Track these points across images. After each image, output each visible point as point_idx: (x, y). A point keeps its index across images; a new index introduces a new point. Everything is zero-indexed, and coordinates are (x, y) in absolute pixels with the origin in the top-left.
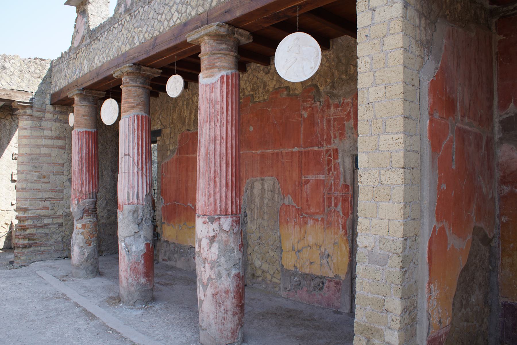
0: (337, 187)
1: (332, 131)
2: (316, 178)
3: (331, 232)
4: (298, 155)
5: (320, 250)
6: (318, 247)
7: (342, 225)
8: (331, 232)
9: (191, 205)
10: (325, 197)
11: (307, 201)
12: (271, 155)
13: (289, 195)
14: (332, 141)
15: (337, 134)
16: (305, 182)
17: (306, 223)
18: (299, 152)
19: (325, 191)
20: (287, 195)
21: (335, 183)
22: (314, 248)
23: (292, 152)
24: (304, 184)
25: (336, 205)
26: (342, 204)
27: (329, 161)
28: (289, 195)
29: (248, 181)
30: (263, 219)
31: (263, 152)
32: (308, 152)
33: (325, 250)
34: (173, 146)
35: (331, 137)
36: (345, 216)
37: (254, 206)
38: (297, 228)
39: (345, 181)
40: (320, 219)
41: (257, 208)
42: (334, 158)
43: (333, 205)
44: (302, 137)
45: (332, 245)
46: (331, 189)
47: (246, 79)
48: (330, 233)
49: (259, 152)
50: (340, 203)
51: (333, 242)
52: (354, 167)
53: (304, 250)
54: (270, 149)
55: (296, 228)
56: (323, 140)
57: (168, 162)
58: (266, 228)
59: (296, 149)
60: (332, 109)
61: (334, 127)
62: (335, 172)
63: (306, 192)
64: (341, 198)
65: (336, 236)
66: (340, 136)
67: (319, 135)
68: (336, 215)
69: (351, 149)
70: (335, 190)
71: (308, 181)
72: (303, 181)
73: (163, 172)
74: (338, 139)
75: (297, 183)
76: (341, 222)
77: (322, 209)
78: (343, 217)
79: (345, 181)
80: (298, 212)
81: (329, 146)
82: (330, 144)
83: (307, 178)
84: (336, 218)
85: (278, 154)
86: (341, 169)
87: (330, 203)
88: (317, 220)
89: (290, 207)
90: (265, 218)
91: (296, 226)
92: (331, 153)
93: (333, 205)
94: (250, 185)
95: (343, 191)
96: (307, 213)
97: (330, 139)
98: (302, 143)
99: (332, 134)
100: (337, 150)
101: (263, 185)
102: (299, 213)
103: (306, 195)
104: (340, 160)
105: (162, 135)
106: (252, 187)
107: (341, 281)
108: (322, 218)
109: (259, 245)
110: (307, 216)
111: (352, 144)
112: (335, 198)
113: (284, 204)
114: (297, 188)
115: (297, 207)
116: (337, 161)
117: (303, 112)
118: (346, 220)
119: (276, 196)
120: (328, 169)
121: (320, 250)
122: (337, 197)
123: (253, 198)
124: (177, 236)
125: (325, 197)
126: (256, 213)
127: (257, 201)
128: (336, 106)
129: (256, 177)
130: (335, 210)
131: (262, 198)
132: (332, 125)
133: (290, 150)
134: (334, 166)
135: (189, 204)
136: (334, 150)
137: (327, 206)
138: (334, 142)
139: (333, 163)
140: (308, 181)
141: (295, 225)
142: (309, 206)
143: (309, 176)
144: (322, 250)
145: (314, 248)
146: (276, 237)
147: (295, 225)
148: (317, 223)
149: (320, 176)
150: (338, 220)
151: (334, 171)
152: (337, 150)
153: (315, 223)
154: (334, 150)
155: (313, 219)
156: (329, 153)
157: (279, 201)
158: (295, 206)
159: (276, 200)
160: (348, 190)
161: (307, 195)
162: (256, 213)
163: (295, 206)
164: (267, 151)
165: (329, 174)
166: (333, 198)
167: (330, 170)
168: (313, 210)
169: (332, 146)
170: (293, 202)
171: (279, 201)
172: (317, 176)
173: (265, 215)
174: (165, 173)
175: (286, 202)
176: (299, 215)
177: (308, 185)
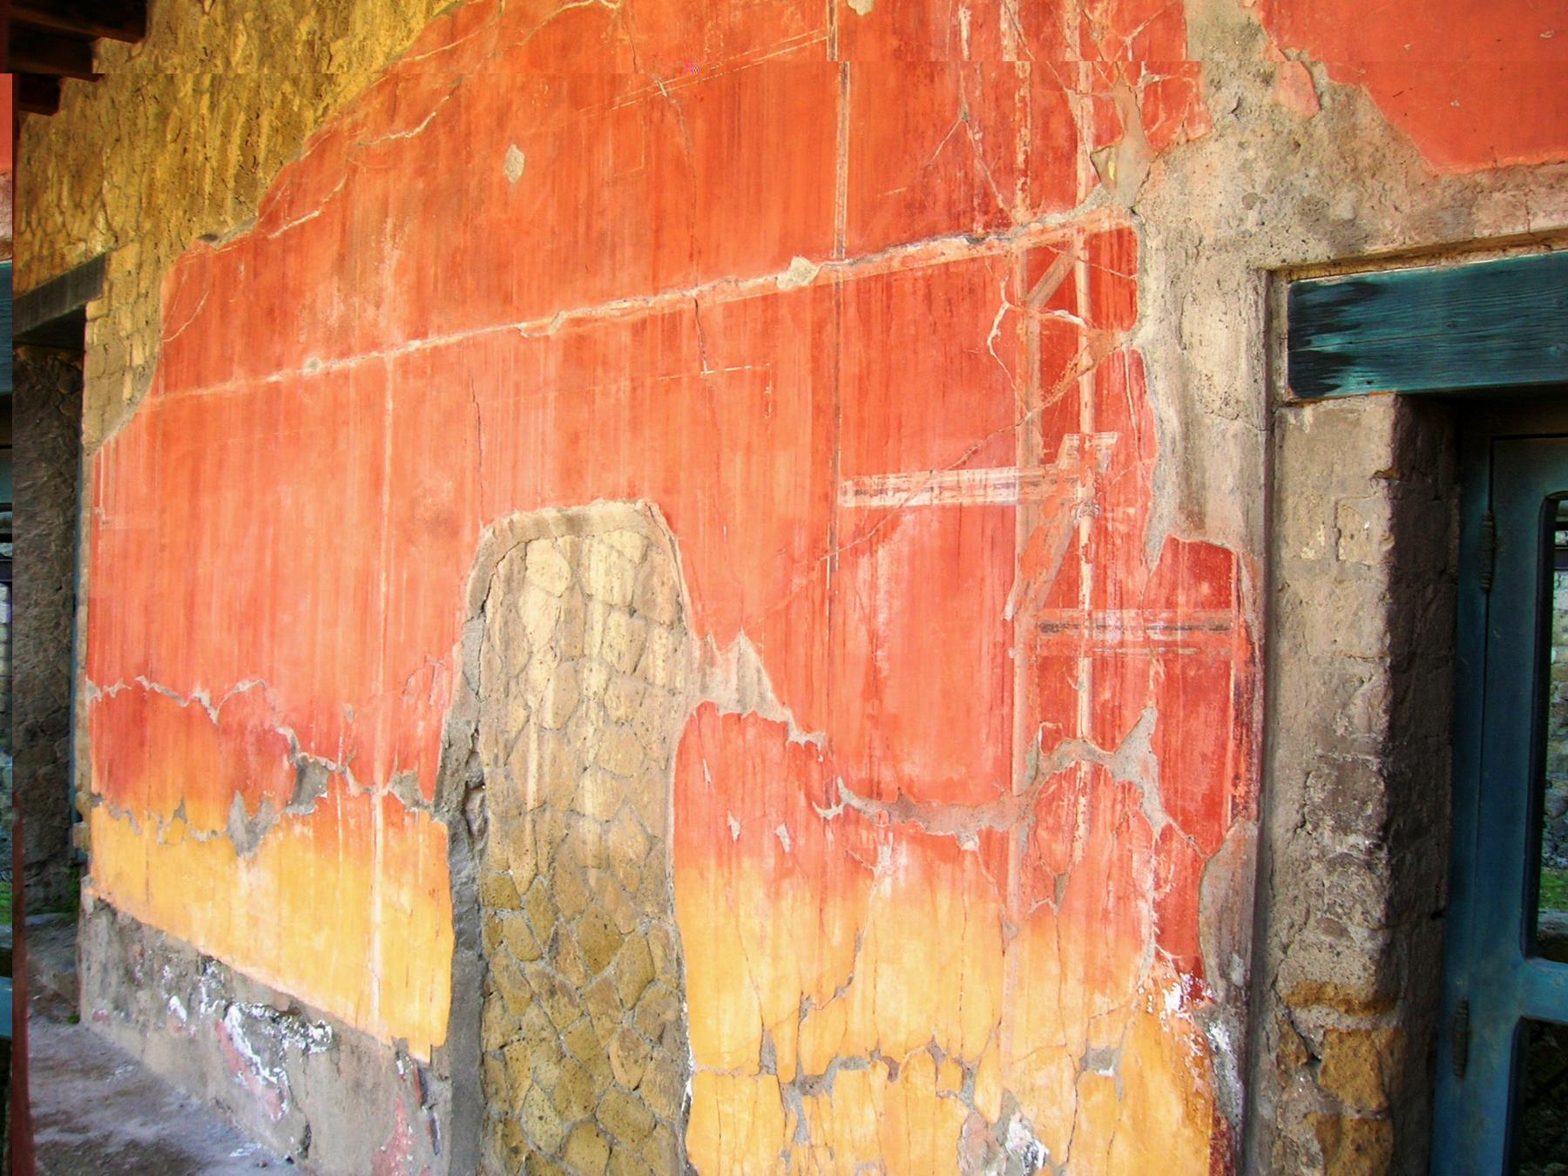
0: (1118, 571)
1: (1083, 85)
2: (948, 499)
3: (1063, 964)
4: (808, 317)
5: (970, 1104)
6: (953, 1074)
7: (1158, 906)
8: (1063, 964)
10: (1017, 654)
11: (873, 687)
12: (626, 337)
14: (1083, 171)
15: (1128, 99)
16: (859, 532)
17: (859, 866)
18: (820, 290)
19: (1019, 605)
20: (726, 638)
21: (1101, 531)
22: (921, 1080)
23: (771, 300)
24: (856, 552)
25: (1109, 728)
26: (1165, 717)
27: (1058, 346)
31: (577, 322)
33: (1009, 1106)
35: (1073, 140)
36: (1186, 825)
37: (522, 714)
38: (797, 908)
39: (1195, 514)
40: (971, 844)
41: (541, 728)
42: (1097, 316)
43: (1083, 724)
44: (842, 171)
45: (1068, 1074)
46: (1066, 590)
48: (1053, 968)
49: (555, 323)
50: (1150, 715)
51: (1076, 1049)
52: (1282, 383)
54: (623, 297)
55: (786, 903)
56: (1007, 170)
57: (117, 442)
59: (798, 273)
62: (1108, 440)
63: (870, 617)
64: (1157, 669)
65: (1101, 1002)
66: (1149, 121)
67: (974, 136)
68: (1104, 818)
69: (1252, 217)
71: (881, 525)
72: (845, 527)
74: (1130, 145)
75: (800, 542)
76: (1148, 883)
77: (990, 752)
78: (1167, 834)
79: (1195, 514)
80: (802, 774)
81: (1054, 218)
83: (876, 502)
84: (1109, 847)
85: (670, 324)
86: (1162, 406)
87: (1056, 705)
88: (948, 850)
89: (751, 733)
91: (786, 884)
92: (1071, 276)
93: (1083, 724)
94: (502, 568)
95: (1171, 604)
96: (872, 790)
97: (1067, 158)
98: (840, 220)
99: (1082, 109)
100: (1123, 239)
101: (576, 562)
103: (863, 635)
104: (1147, 333)
108: (987, 837)
109: (552, 993)
110: (872, 809)
111: (1262, 173)
112: (1100, 667)
113: (706, 708)
114: (798, 582)
115: (797, 736)
116: (1121, 337)
118: (1197, 868)
119: (660, 641)
120: (1047, 414)
121: (970, 1104)
122: (1120, 662)
123: (521, 659)
125: (1017, 654)
126: (533, 767)
129: (534, 507)
130: (1097, 771)
131: (572, 657)
133: (753, 284)
136: (1094, 243)
137: (1029, 737)
138: (1099, 177)
143: (892, 480)
144: (979, 1099)
145: (921, 1080)
148: (945, 870)
149: (979, 475)
150: (1124, 863)
151: (1099, 427)
152: (1123, 239)
153: (929, 876)
154: (1094, 243)
155: (921, 841)
156: (1057, 273)
158: (784, 728)
159: (660, 677)
160: (1221, 599)
162: (533, 767)
163: (784, 728)
164: (601, 311)
165: (1050, 458)
166: (1084, 666)
167: (1059, 421)
168: (917, 766)
169: (1079, 214)
170: (771, 695)
171: (679, 683)
172: (950, 478)
176: (809, 797)
177: (882, 553)
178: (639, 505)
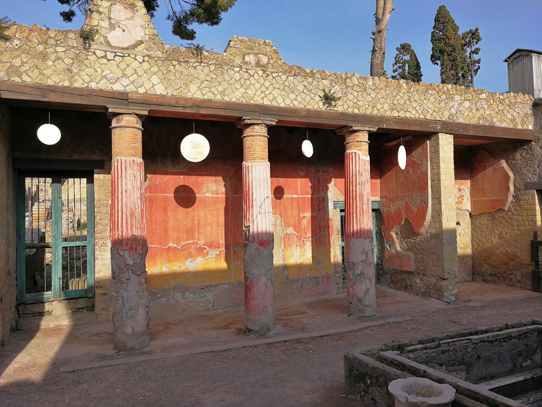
9: (175, 245)
10: (317, 227)
13: (291, 227)
18: (298, 198)
20: (289, 227)
23: (292, 198)
24: (302, 219)
28: (291, 227)
32: (304, 198)
43: (322, 231)
55: (297, 249)
60: (321, 173)
61: (322, 185)
62: (323, 211)
65: (325, 250)
70: (323, 222)
71: (305, 217)
75: (297, 219)
77: (315, 234)
81: (319, 195)
82: (320, 194)
93: (322, 231)
96: (305, 238)
99: (321, 188)
107: (330, 276)
110: (305, 240)
112: (323, 227)
114: (297, 222)
115: (297, 235)
128: (324, 172)
132: (321, 183)
134: (322, 207)
139: (321, 206)
140: (305, 217)
141: (296, 247)
142: (306, 233)
143: (305, 214)
147: (296, 247)
150: (326, 239)
161: (305, 226)
166: (322, 227)
167: (319, 210)
177: (305, 219)
178: (277, 215)
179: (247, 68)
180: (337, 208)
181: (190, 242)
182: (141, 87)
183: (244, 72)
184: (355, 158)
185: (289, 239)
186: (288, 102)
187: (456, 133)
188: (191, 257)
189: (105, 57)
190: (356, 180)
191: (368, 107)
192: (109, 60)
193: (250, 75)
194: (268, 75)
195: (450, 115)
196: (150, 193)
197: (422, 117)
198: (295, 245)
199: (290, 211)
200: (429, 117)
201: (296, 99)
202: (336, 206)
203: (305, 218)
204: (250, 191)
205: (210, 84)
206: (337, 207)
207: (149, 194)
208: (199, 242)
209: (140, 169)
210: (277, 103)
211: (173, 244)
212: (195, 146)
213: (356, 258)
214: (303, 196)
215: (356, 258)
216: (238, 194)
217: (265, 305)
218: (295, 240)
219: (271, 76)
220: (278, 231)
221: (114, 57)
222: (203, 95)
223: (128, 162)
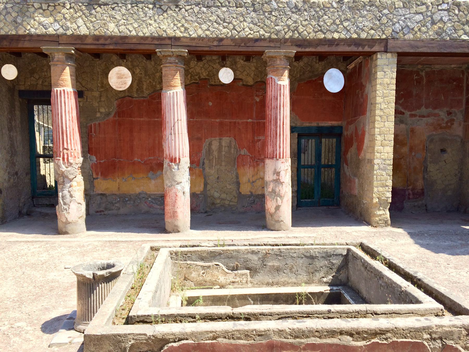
9: (139, 160)
17: (258, 165)
20: (242, 149)
23: (247, 122)
29: (206, 140)
30: (221, 165)
34: (105, 109)
37: (212, 157)
38: (252, 169)
47: (201, 66)
49: (218, 120)
53: (257, 181)
57: (99, 124)
58: (224, 171)
63: (258, 147)
73: (91, 132)
75: (251, 141)
90: (223, 164)
96: (259, 159)
101: (220, 142)
102: (253, 159)
105: (85, 97)
106: (210, 144)
110: (259, 160)
117: (256, 98)
123: (212, 152)
124: (119, 188)
126: (214, 161)
127: (216, 154)
135: (136, 159)
140: (260, 140)
141: (250, 166)
146: (233, 176)
147: (250, 166)
157: (235, 153)
159: (233, 152)
161: (259, 148)
162: (214, 161)
173: (223, 162)
174: (95, 132)
175: (242, 153)
179: (160, 4)
180: (295, 132)
181: (152, 158)
182: (68, 30)
183: (158, 8)
184: (272, 83)
185: (243, 160)
186: (200, 32)
187: (400, 51)
188: (153, 170)
189: (41, 8)
190: (271, 104)
191: (288, 31)
192: (44, 10)
193: (163, 10)
194: (181, 9)
195: (393, 31)
196: (119, 117)
197: (355, 36)
198: (248, 166)
199: (245, 134)
200: (364, 35)
201: (208, 30)
202: (294, 130)
203: (259, 141)
204: (164, 115)
205: (126, 22)
206: (294, 131)
207: (118, 118)
208: (159, 158)
209: (71, 97)
210: (189, 34)
211: (138, 159)
212: (120, 77)
213: (269, 177)
214: (258, 121)
215: (269, 177)
216: (194, 119)
217: (176, 210)
218: (248, 160)
219: (183, 10)
220: (233, 152)
221: (48, 7)
222: (120, 32)
223: (59, 92)
